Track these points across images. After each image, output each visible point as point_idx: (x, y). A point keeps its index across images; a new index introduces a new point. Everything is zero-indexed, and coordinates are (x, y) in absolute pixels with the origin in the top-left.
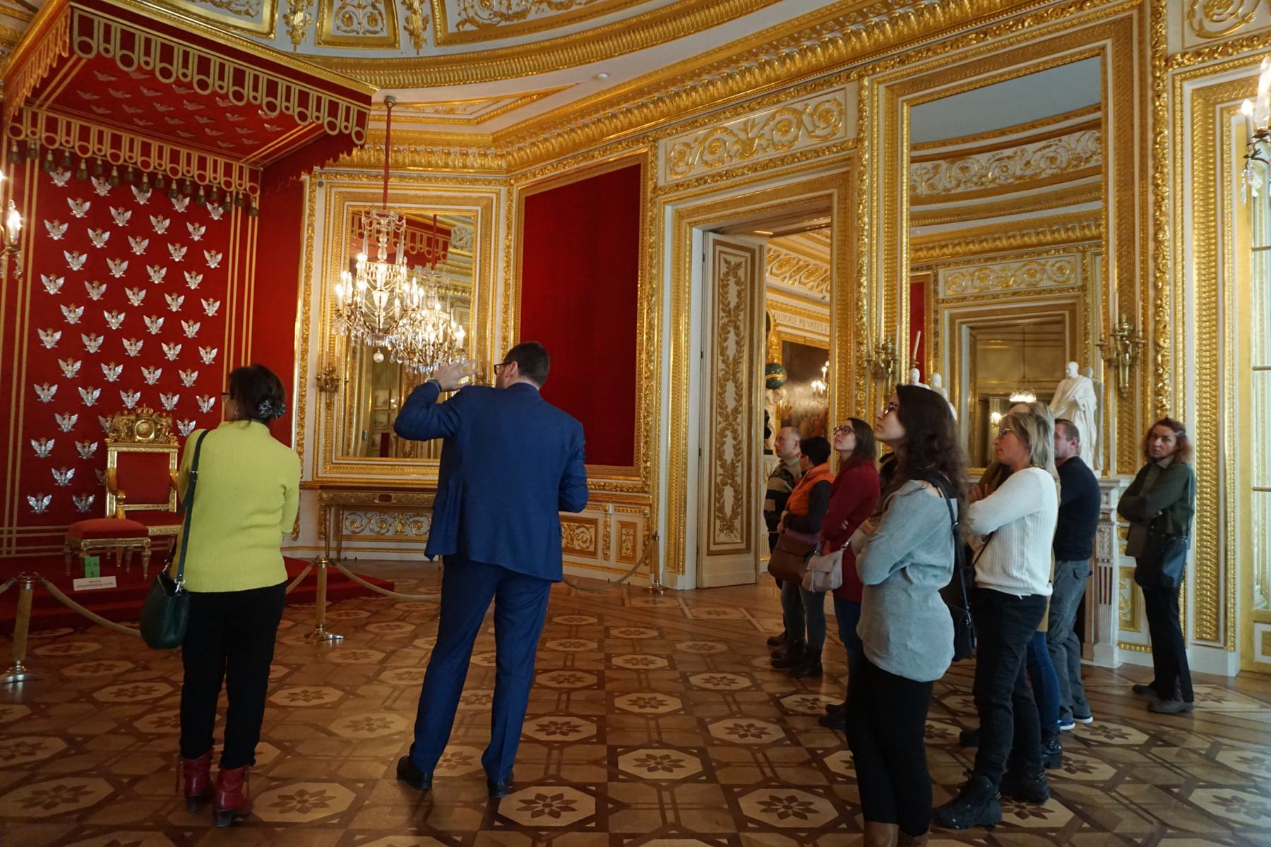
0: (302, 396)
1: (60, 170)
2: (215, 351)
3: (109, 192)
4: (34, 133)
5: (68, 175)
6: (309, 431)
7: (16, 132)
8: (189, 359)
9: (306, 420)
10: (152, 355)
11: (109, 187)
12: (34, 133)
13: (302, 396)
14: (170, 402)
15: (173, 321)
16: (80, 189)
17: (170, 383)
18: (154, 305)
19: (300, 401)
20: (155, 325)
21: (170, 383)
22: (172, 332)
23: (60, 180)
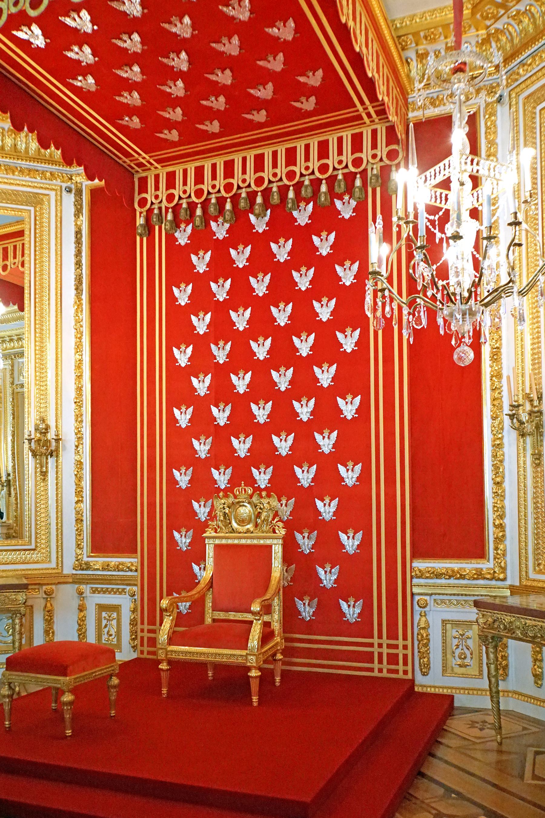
0: (498, 446)
1: (183, 226)
2: (358, 399)
3: (228, 232)
4: (157, 197)
5: (189, 228)
6: (510, 504)
7: (143, 202)
8: (326, 416)
9: (506, 485)
10: (283, 419)
11: (227, 226)
12: (157, 197)
13: (498, 446)
14: (305, 476)
15: (303, 367)
16: (202, 239)
17: (305, 451)
18: (282, 354)
19: (495, 456)
20: (282, 379)
21: (305, 451)
22: (304, 385)
23: (182, 238)
